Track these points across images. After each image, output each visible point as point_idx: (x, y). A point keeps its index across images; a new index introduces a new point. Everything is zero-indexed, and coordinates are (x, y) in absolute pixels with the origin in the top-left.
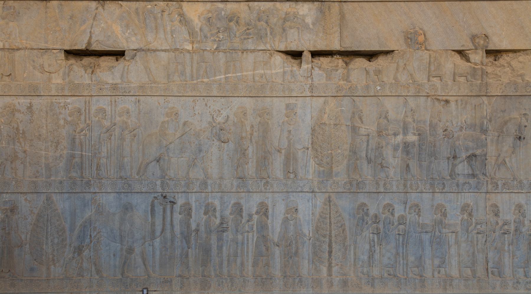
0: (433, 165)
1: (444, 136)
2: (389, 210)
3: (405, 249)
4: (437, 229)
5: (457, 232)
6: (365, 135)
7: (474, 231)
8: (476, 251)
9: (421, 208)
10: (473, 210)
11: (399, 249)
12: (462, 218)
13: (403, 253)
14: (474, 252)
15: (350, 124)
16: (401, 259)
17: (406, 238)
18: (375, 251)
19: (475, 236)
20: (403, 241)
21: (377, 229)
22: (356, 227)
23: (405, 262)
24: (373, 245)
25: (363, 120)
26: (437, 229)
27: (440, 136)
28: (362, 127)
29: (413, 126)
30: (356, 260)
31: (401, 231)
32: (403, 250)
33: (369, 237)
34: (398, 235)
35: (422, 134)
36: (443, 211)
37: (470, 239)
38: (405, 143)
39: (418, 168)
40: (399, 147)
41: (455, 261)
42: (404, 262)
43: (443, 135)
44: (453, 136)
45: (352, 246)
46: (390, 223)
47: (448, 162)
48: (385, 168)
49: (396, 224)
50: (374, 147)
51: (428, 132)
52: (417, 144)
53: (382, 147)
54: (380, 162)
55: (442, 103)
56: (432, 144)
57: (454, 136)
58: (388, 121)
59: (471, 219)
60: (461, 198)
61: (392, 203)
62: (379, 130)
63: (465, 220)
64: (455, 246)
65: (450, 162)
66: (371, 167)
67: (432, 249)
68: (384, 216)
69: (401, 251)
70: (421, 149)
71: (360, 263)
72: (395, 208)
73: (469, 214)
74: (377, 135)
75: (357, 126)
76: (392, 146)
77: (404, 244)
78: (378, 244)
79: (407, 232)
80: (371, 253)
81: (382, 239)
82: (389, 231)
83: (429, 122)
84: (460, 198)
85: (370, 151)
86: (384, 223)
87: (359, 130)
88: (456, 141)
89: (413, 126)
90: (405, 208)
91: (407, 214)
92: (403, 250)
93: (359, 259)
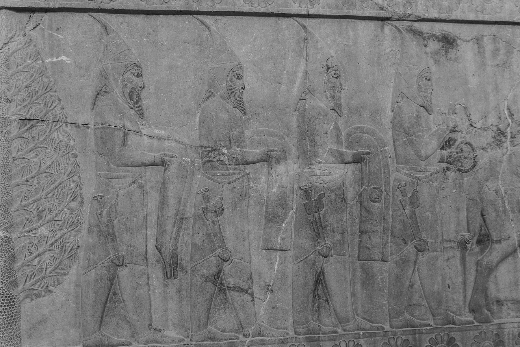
0: (411, 271)
1: (445, 165)
6: (152, 165)
15: (92, 123)
25: (145, 103)
27: (430, 164)
28: (139, 133)
29: (337, 128)
35: (368, 157)
38: (307, 192)
39: (358, 287)
40: (285, 206)
43: (441, 161)
44: (475, 165)
47: (463, 259)
48: (235, 294)
50: (190, 212)
51: (390, 149)
52: (351, 193)
53: (220, 211)
54: (213, 270)
55: (433, 46)
56: (404, 194)
57: (479, 164)
58: (243, 109)
62: (205, 143)
65: (468, 258)
66: (179, 291)
70: (369, 212)
74: (198, 162)
75: (118, 128)
76: (260, 204)
83: (389, 114)
85: (170, 228)
87: (124, 143)
88: (487, 180)
89: (337, 128)
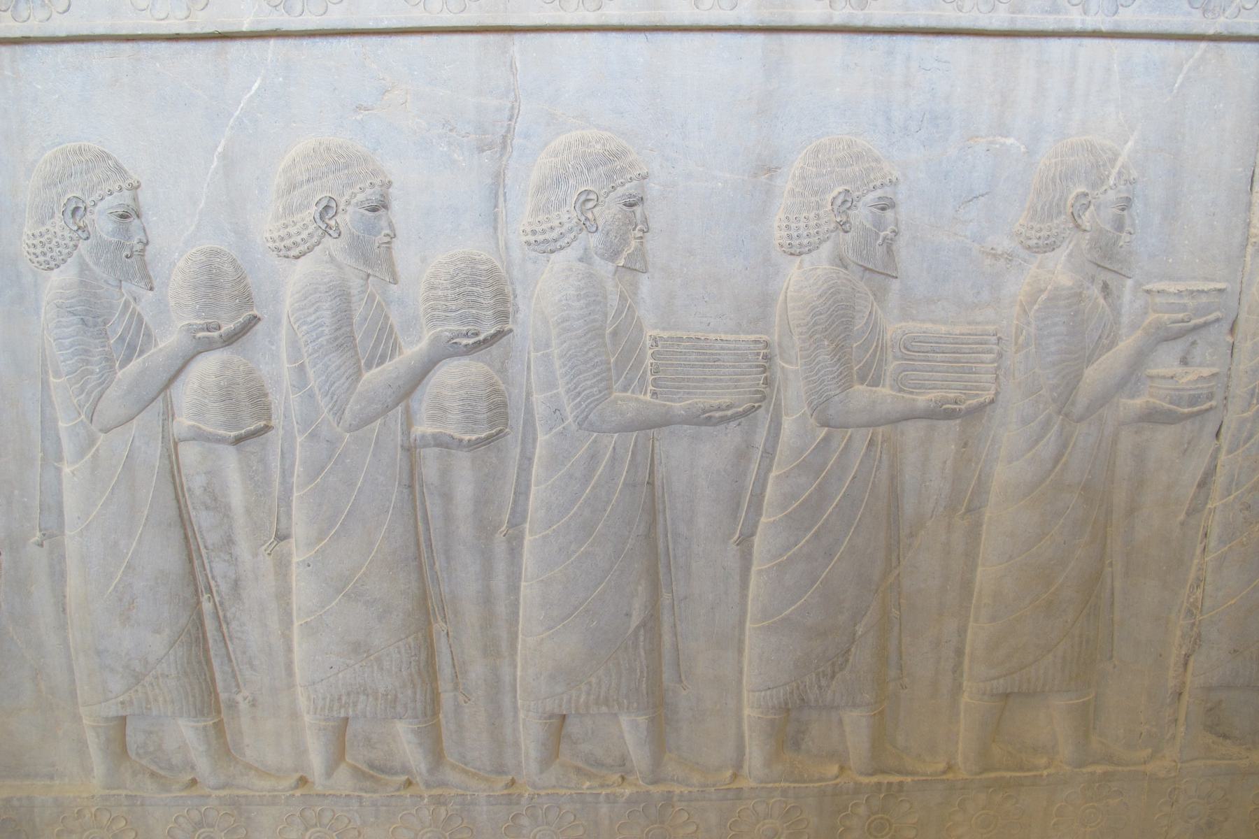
3: (501, 567)
10: (1138, 206)
13: (487, 599)
18: (236, 585)
20: (483, 501)
32: (487, 573)
59: (1105, 287)
80: (207, 606)
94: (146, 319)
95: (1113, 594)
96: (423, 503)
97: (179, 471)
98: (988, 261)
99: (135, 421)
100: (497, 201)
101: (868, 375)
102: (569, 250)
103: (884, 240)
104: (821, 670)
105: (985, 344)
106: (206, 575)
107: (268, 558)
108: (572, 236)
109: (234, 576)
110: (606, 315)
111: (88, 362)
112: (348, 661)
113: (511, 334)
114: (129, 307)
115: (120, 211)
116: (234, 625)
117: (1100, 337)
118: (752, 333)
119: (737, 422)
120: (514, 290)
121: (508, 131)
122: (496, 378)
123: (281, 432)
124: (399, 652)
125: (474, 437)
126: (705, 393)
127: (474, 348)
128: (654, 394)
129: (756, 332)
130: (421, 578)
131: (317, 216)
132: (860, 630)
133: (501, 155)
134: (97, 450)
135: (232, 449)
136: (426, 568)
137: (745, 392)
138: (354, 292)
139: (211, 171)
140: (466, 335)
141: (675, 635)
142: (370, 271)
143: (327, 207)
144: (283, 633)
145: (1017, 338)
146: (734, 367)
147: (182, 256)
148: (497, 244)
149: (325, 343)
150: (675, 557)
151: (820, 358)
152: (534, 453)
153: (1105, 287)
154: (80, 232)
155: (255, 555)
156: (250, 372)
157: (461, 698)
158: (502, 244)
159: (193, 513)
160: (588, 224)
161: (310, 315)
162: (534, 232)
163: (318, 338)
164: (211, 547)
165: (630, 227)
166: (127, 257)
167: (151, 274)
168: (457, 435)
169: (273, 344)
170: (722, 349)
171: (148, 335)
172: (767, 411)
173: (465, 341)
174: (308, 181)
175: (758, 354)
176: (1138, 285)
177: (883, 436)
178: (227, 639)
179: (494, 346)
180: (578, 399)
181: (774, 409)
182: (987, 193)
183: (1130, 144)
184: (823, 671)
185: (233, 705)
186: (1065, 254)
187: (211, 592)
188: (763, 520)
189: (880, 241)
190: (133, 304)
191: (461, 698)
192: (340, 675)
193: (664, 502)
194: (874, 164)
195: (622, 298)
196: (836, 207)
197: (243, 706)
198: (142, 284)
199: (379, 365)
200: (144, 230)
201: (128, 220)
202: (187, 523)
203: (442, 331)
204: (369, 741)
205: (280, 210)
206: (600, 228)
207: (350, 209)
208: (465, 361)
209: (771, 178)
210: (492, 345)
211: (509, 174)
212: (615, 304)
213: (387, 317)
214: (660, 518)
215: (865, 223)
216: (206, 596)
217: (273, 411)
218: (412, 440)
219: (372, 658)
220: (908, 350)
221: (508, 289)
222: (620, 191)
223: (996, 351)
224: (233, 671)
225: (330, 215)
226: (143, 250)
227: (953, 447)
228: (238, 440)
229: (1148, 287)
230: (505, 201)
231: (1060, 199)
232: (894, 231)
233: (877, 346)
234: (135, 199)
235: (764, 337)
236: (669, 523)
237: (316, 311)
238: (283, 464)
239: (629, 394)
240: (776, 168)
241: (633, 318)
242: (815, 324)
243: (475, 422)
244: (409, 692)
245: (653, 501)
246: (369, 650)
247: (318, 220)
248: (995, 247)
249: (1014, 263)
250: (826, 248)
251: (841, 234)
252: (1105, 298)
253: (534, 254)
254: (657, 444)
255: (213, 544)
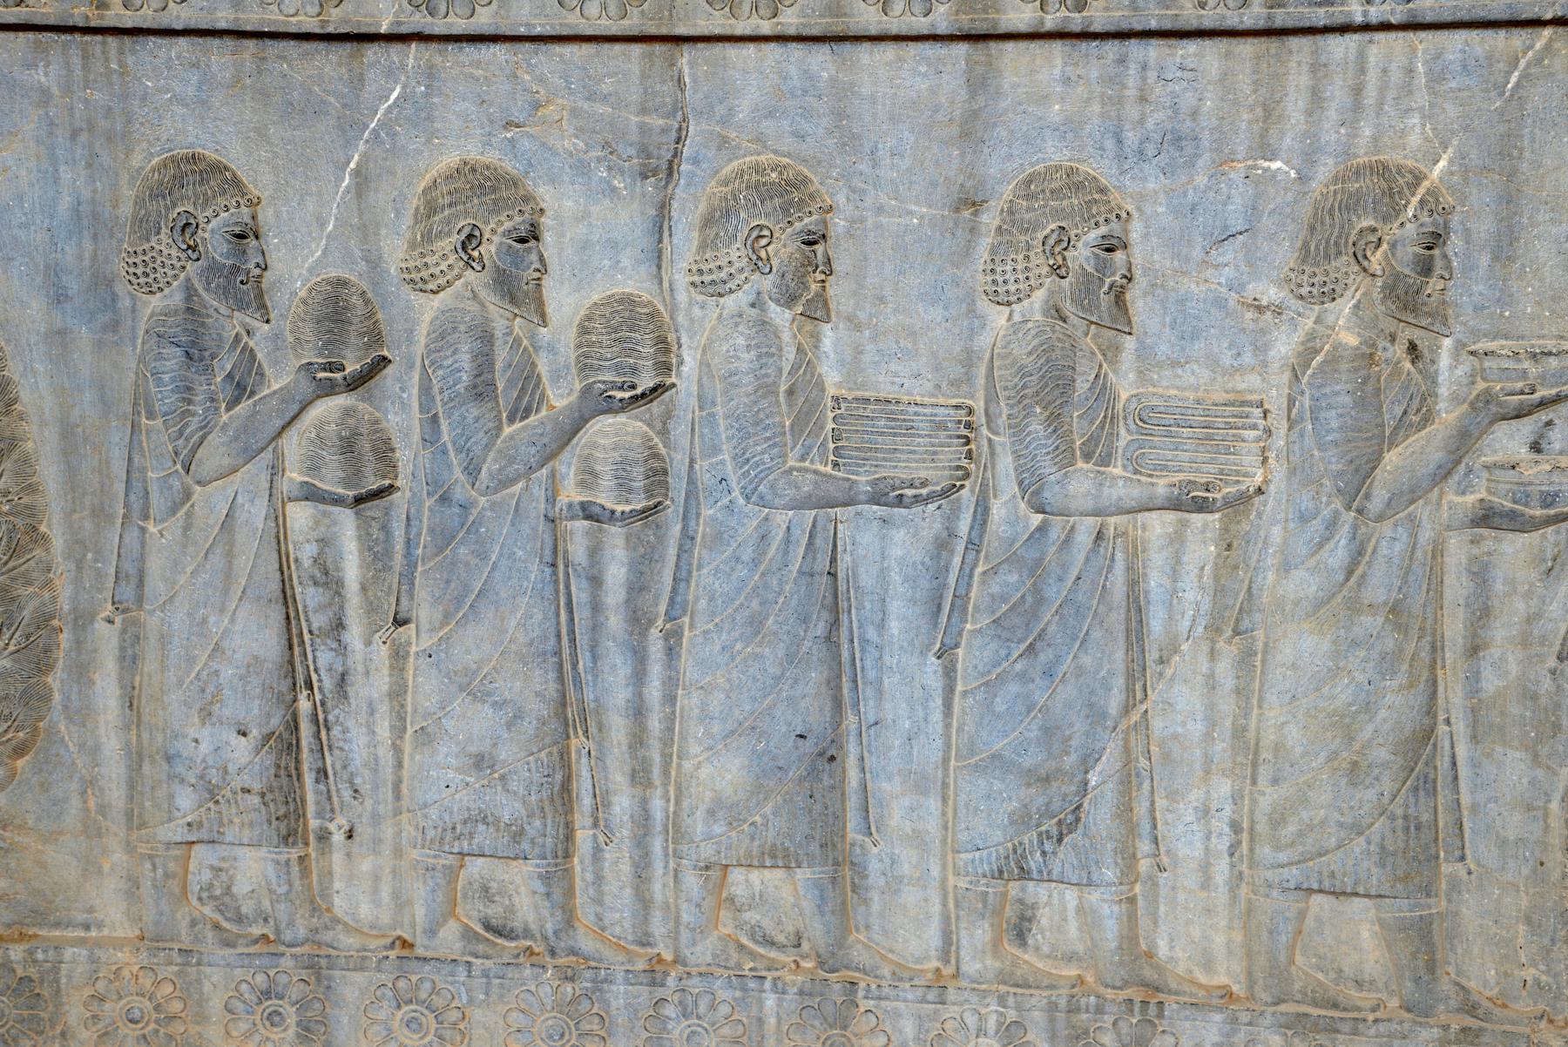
2: (470, 240)
3: (656, 669)
4: (1006, 463)
5: (1241, 502)
7: (1452, 497)
8: (1460, 727)
9: (838, 224)
10: (1455, 243)
11: (595, 671)
12: (1311, 336)
13: (638, 711)
14: (1426, 735)
16: (619, 778)
17: (672, 551)
18: (342, 680)
19: (1457, 551)
20: (638, 586)
21: (348, 446)
22: (135, 426)
23: (657, 804)
24: (319, 621)
26: (1006, 463)
30: (146, 767)
31: (607, 482)
32: (639, 676)
33: (279, 537)
34: (581, 525)
36: (1081, 255)
37: (1378, 588)
41: (1205, 812)
42: (644, 804)
45: (100, 626)
46: (482, 390)
49: (560, 397)
59: (1413, 348)
60: (1316, 98)
61: (510, 166)
63: (1333, 360)
64: (1213, 654)
67: (949, 673)
68: (428, 309)
69: (620, 695)
71: (186, 800)
72: (546, 221)
73: (1390, 291)
77: (651, 622)
78: (371, 608)
79: (678, 486)
80: (304, 705)
81: (411, 566)
82: (472, 471)
84: (1295, 108)
86: (426, 390)
90: (661, 223)
91: (682, 297)
92: (639, 676)
93: (169, 759)
94: (259, 356)
95: (1454, 764)
96: (568, 586)
97: (285, 538)
98: (1249, 315)
99: (239, 474)
100: (661, 236)
101: (1094, 452)
102: (740, 294)
103: (1111, 288)
104: (1043, 828)
105: (1247, 417)
106: (308, 666)
107: (384, 648)
108: (743, 277)
109: (340, 669)
110: (780, 370)
111: (190, 402)
112: (468, 779)
113: (674, 390)
114: (240, 341)
115: (237, 230)
116: (336, 731)
117: (1405, 412)
118: (953, 397)
119: (936, 504)
120: (679, 339)
121: (675, 155)
122: (656, 440)
123: (408, 494)
124: (529, 770)
125: (627, 508)
126: (896, 467)
127: (630, 404)
128: (836, 465)
129: (959, 397)
130: (561, 679)
131: (459, 247)
132: (1093, 779)
133: (667, 183)
134: (192, 506)
135: (348, 512)
136: (567, 666)
137: (944, 468)
138: (498, 334)
139: (342, 189)
140: (621, 388)
141: (863, 770)
142: (516, 311)
143: (470, 237)
144: (393, 744)
145: (1289, 411)
146: (930, 436)
147: (304, 285)
148: (661, 283)
149: (462, 391)
150: (863, 668)
151: (1031, 428)
152: (696, 532)
153: (1413, 348)
154: (190, 252)
155: (368, 643)
156: (377, 422)
157: (601, 838)
158: (666, 284)
159: (298, 590)
160: (760, 264)
161: (447, 357)
162: (700, 272)
163: (455, 385)
164: (316, 632)
165: (810, 269)
166: (242, 282)
167: (269, 304)
168: (609, 505)
169: (404, 391)
170: (916, 414)
171: (261, 374)
172: (972, 491)
173: (619, 395)
174: (450, 205)
175: (959, 422)
176: (1460, 346)
177: (1115, 529)
178: (326, 748)
179: (655, 403)
180: (747, 467)
181: (980, 490)
182: (1246, 231)
183: (1442, 164)
184: (1047, 832)
185: (324, 836)
186: (1350, 305)
187: (311, 689)
188: (968, 626)
189: (1106, 288)
190: (245, 338)
191: (601, 838)
192: (457, 797)
193: (849, 599)
194: (1097, 196)
195: (800, 350)
196: (1048, 248)
197: (338, 837)
198: (258, 315)
199: (523, 419)
200: (263, 253)
201: (246, 241)
202: (290, 601)
203: (595, 382)
204: (487, 892)
205: (419, 237)
206: (774, 269)
207: (496, 239)
208: (622, 418)
209: (976, 213)
210: (651, 401)
211: (675, 205)
212: (792, 356)
213: (534, 365)
214: (844, 618)
215: (1087, 267)
216: (305, 693)
217: (400, 469)
218: (557, 510)
219: (496, 775)
220: (1145, 423)
221: (671, 337)
222: (798, 226)
223: (1261, 427)
224: (329, 791)
225: (474, 245)
226: (260, 276)
227: (1212, 548)
228: (359, 500)
229: (1473, 348)
230: (670, 235)
231: (1340, 237)
232: (1126, 277)
233: (1105, 417)
234: (254, 218)
235: (969, 402)
236: (855, 625)
237: (454, 353)
238: (407, 533)
239: (807, 464)
240: (983, 201)
241: (813, 376)
242: (1024, 387)
243: (630, 490)
244: (538, 823)
245: (836, 597)
246: (493, 765)
247: (460, 251)
248: (1258, 296)
249: (1284, 317)
250: (1040, 295)
251: (1057, 279)
252: (1413, 362)
253: (703, 297)
254: (840, 526)
255: (320, 628)
